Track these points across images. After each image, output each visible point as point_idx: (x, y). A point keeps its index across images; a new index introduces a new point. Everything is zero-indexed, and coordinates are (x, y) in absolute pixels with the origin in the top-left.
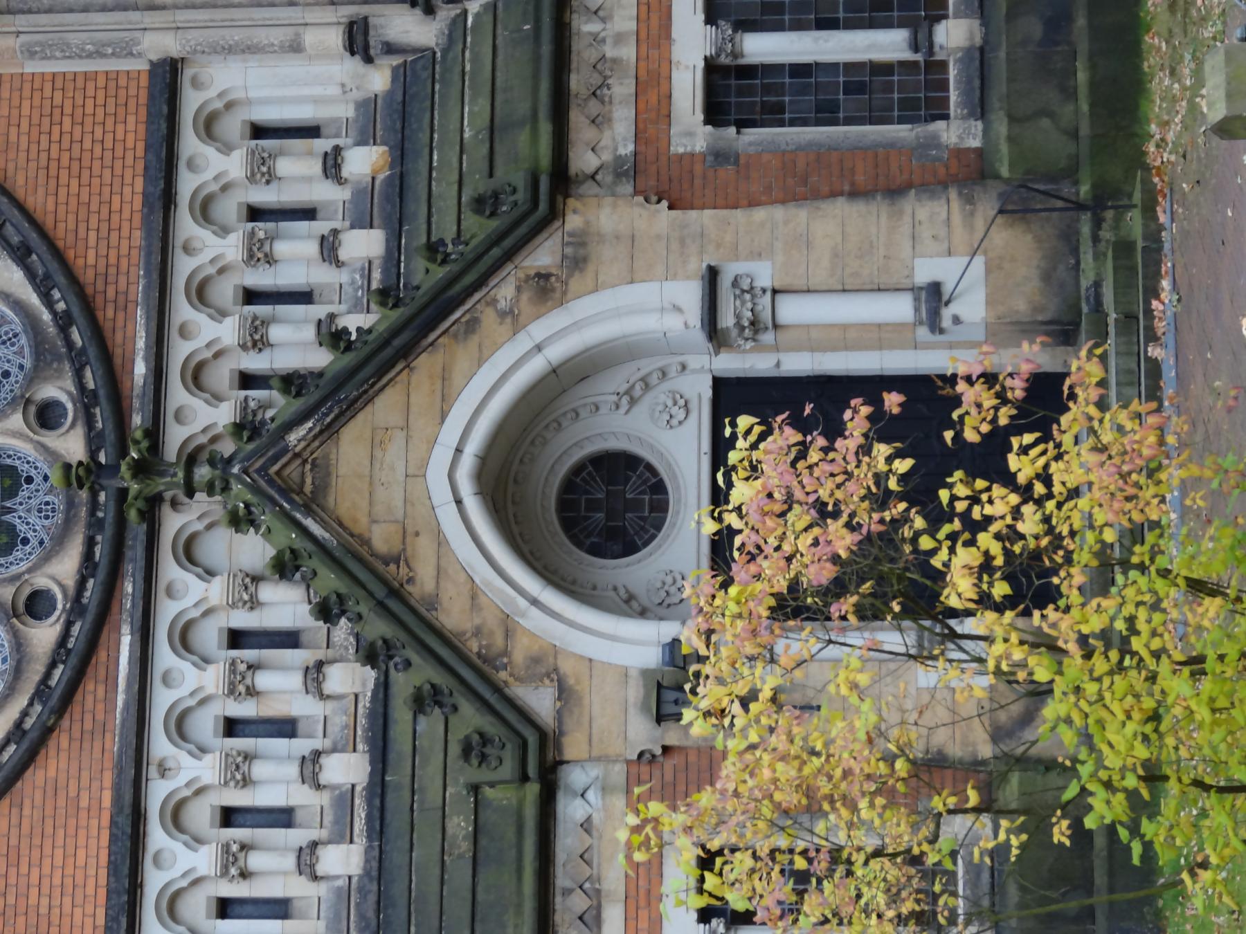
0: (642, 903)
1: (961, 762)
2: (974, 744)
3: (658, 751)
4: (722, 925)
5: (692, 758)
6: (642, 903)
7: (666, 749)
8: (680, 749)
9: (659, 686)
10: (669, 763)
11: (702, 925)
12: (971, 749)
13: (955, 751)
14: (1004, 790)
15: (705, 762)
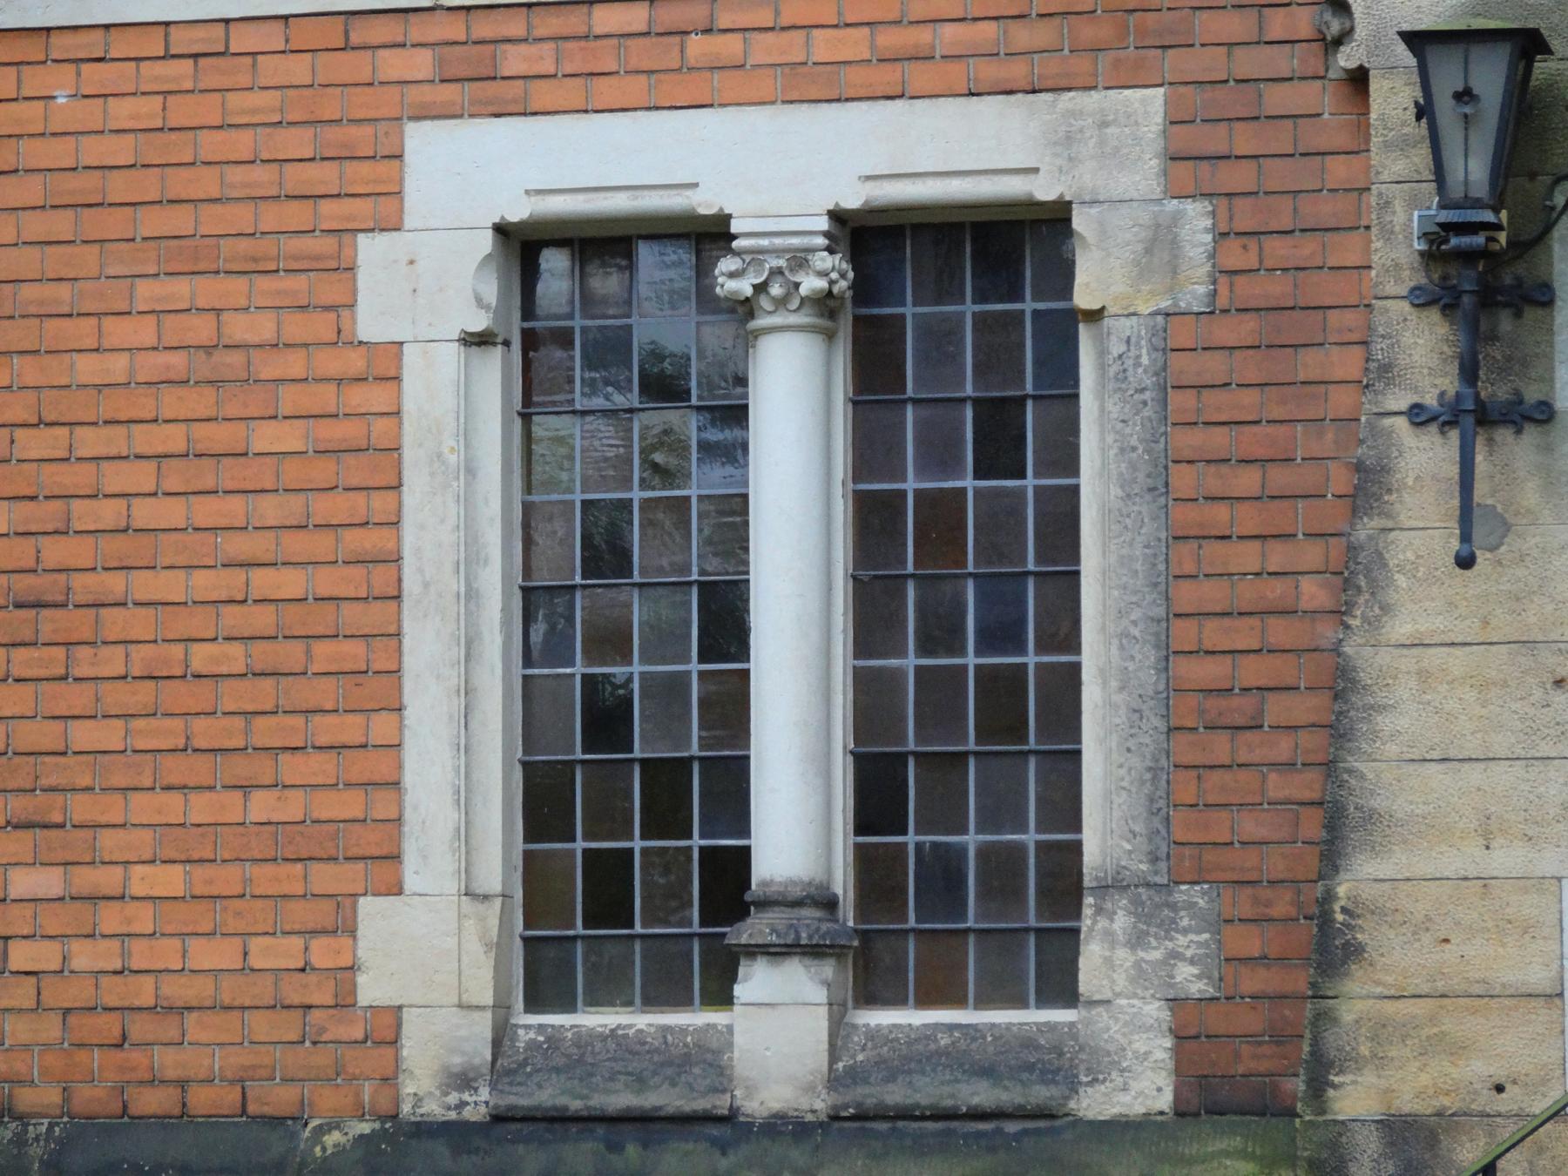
0: (890, 39)
1: (1323, 1019)
2: (1379, 1061)
3: (1347, 58)
4: (822, 284)
5: (1339, 170)
6: (890, 39)
7: (1359, 79)
8: (1362, 128)
9: (1528, 44)
10: (1324, 99)
11: (823, 224)
12: (1364, 1050)
13: (1357, 1001)
14: (1243, 1155)
15: (1326, 210)
